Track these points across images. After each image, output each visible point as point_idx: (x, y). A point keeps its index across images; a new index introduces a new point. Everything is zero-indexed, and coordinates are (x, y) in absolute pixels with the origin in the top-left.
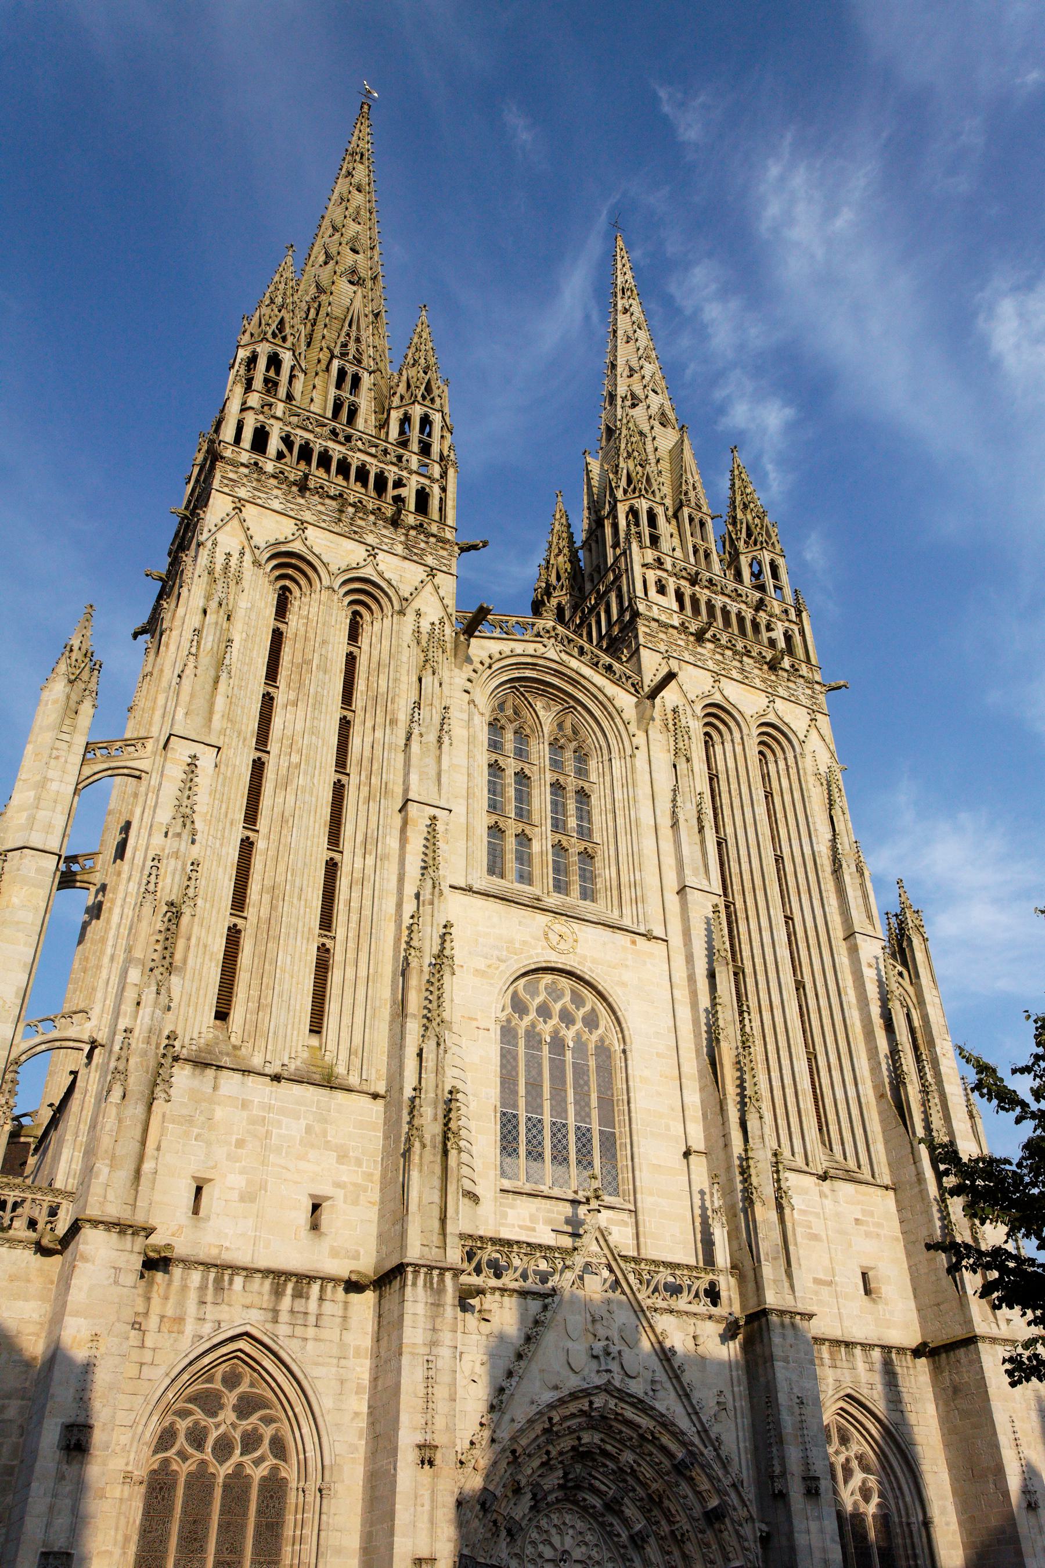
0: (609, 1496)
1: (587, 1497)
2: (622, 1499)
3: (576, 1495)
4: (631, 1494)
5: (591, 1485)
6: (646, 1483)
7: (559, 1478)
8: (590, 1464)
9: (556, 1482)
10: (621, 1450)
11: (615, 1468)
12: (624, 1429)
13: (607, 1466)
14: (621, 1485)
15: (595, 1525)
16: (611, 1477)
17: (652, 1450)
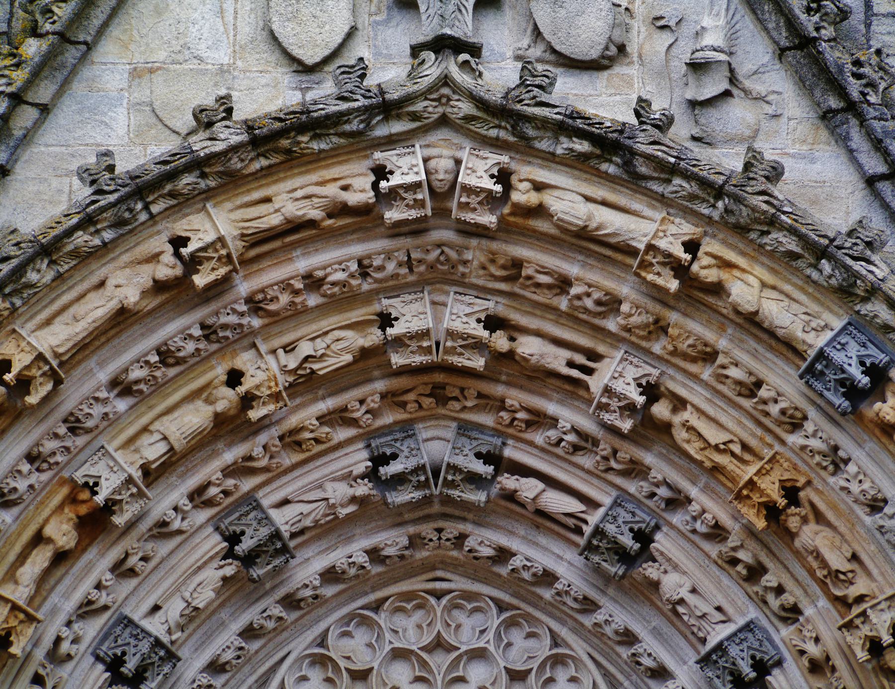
0: (588, 530)
1: (513, 544)
2: (644, 538)
3: (462, 538)
4: (677, 518)
5: (511, 496)
6: (716, 470)
7: (349, 478)
8: (487, 419)
9: (339, 492)
10: (594, 356)
11: (588, 425)
12: (572, 269)
13: (553, 422)
14: (632, 487)
15: (579, 647)
16: (587, 461)
17: (710, 336)
